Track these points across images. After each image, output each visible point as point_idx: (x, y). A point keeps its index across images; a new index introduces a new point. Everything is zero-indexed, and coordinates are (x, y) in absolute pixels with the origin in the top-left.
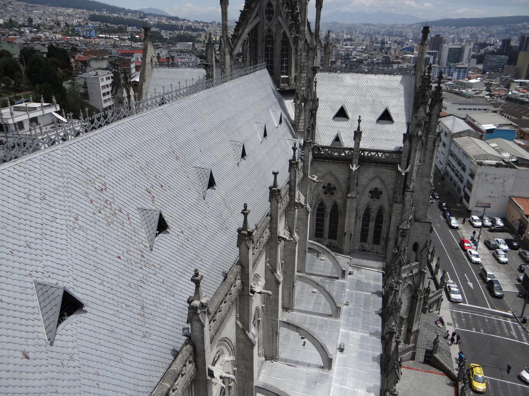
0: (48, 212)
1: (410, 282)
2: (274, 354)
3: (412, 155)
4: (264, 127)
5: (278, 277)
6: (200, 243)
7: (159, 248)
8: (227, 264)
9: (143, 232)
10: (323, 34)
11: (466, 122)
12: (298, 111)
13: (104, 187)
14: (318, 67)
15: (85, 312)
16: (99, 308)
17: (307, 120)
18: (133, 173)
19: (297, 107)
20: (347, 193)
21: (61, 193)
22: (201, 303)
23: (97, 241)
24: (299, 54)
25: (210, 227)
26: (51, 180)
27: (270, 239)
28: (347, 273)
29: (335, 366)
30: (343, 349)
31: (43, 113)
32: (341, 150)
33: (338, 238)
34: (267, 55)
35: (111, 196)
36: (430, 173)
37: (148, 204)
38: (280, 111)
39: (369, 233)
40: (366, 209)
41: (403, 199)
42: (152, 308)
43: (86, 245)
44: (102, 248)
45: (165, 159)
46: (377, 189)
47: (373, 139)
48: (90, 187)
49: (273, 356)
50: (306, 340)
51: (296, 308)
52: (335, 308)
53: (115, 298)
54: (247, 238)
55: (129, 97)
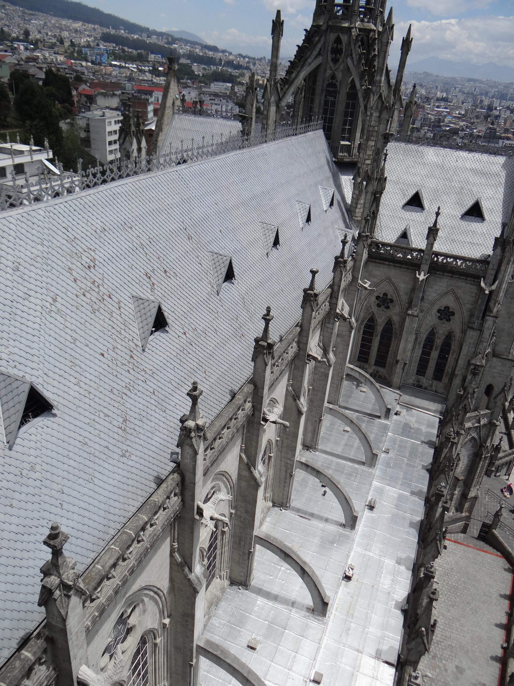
0: (21, 287)
1: (474, 435)
2: (285, 501)
3: (503, 268)
4: (308, 210)
5: (300, 406)
6: (206, 349)
7: (154, 349)
8: (237, 380)
9: (137, 328)
10: (406, 89)
12: (357, 192)
13: (92, 264)
14: (392, 135)
15: (55, 415)
16: (72, 413)
17: (367, 205)
18: (131, 250)
19: (357, 187)
20: (407, 309)
21: (38, 265)
22: (197, 425)
23: (78, 331)
24: (369, 113)
25: (220, 331)
26: (28, 247)
27: (296, 356)
28: (392, 412)
29: (360, 526)
30: (373, 507)
31: (32, 158)
33: (387, 365)
34: (325, 112)
35: (100, 276)
37: (145, 292)
38: (332, 190)
39: (430, 364)
40: (430, 332)
41: (482, 325)
42: (136, 422)
43: (63, 334)
44: (83, 340)
45: (174, 236)
46: (449, 308)
48: (75, 262)
49: (283, 503)
50: (327, 489)
51: (320, 447)
52: (370, 454)
53: (92, 403)
54: (265, 351)
55: (139, 150)
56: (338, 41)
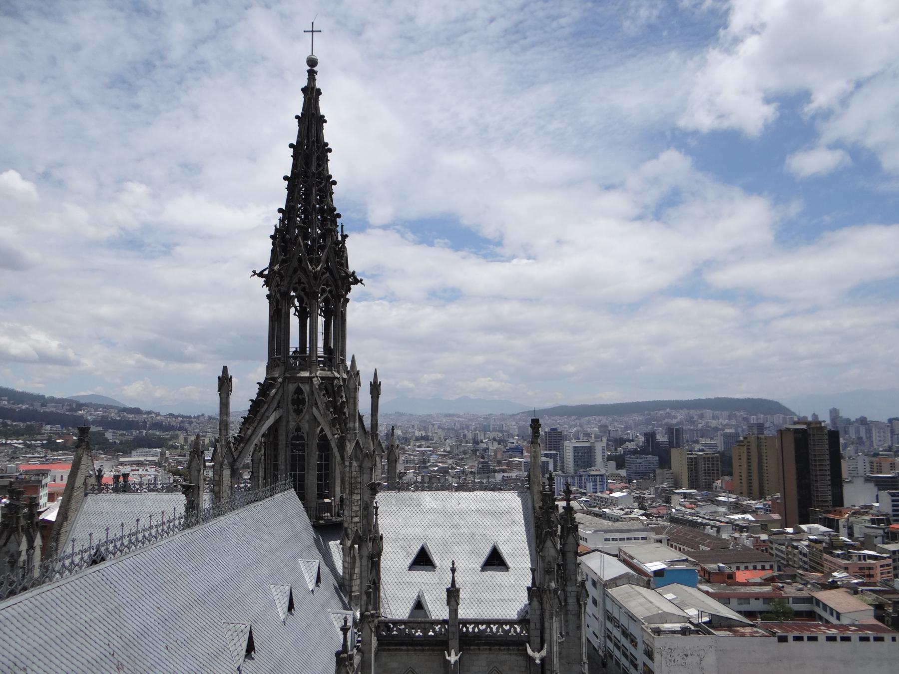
3: (547, 625)
4: (288, 593)
11: (620, 560)
12: (348, 559)
14: (379, 484)
19: (347, 552)
24: (347, 464)
32: (427, 626)
36: (581, 654)
38: (316, 562)
47: (480, 601)
56: (299, 391)
